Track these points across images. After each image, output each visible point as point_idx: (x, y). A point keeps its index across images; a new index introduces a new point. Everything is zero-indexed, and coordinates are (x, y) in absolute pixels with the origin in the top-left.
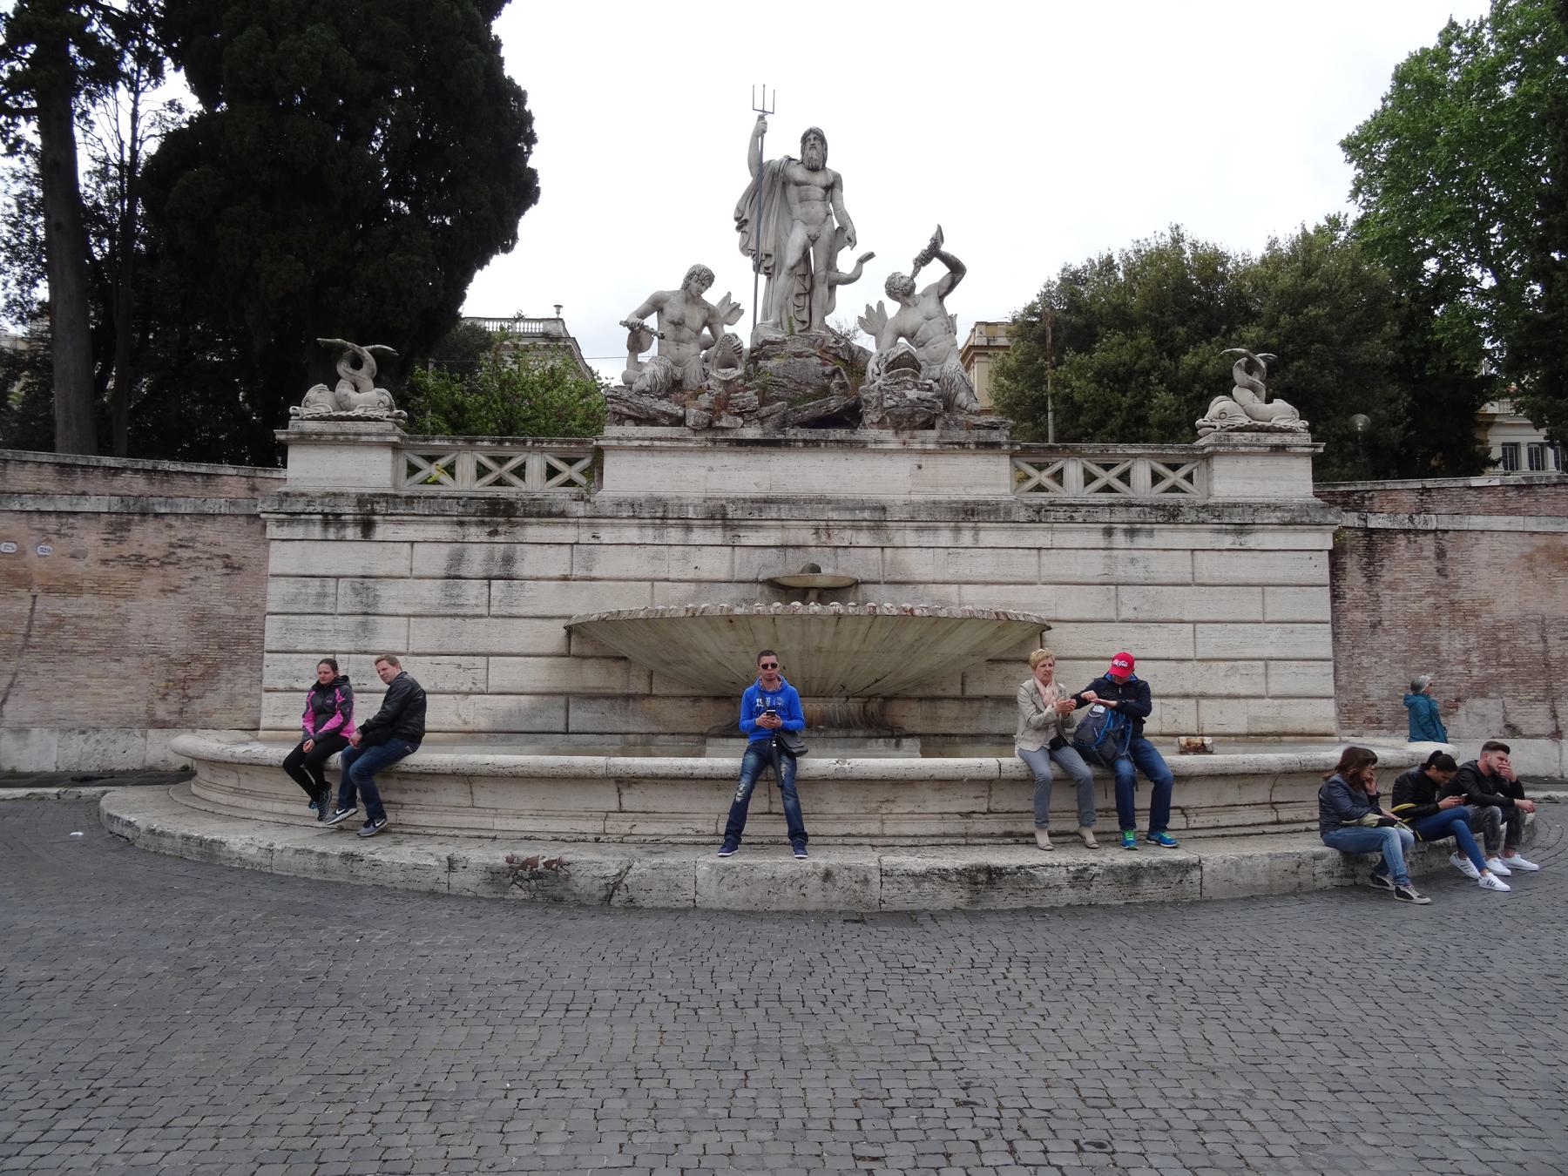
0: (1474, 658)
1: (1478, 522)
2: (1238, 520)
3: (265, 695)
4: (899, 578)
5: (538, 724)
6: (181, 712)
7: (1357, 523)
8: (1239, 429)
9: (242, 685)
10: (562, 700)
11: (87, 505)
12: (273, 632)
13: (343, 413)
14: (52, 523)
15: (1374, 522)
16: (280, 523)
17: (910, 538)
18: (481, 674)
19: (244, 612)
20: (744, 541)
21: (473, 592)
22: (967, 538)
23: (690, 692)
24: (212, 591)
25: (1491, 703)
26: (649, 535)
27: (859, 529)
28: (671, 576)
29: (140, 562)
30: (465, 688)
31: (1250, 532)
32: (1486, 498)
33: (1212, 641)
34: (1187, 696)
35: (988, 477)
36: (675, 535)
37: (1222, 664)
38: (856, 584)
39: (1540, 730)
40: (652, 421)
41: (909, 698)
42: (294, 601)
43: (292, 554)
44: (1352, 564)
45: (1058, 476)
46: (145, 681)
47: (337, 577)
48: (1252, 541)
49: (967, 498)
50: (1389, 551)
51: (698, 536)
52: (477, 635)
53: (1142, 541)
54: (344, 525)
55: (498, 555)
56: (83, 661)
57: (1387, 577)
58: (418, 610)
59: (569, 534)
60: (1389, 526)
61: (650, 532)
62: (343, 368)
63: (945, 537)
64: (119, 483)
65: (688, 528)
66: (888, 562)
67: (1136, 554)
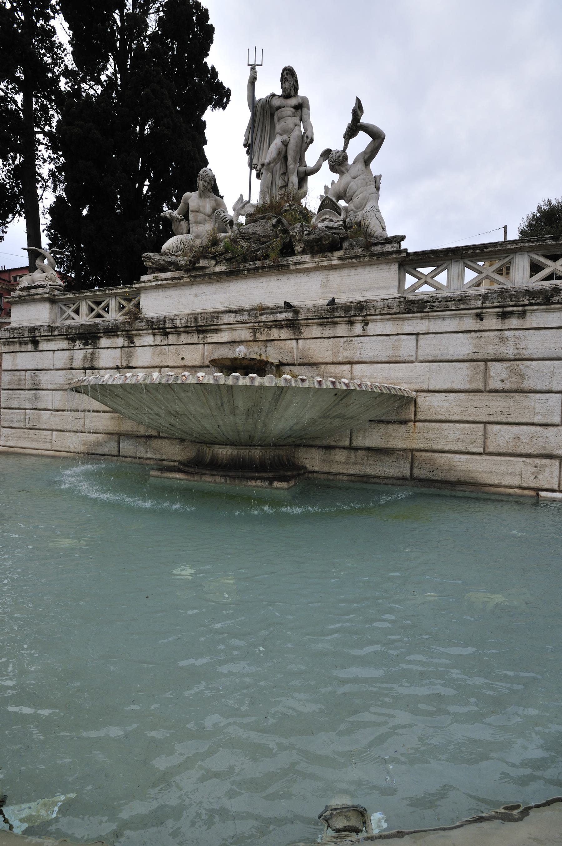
5: (104, 450)
10: (116, 437)
17: (315, 331)
20: (210, 340)
22: (358, 329)
26: (159, 340)
28: (170, 364)
36: (172, 339)
41: (311, 446)
42: (9, 383)
47: (26, 370)
49: (362, 299)
51: (184, 338)
53: (514, 322)
55: (89, 356)
58: (55, 387)
61: (159, 338)
65: (179, 334)
66: (300, 350)
67: (507, 333)
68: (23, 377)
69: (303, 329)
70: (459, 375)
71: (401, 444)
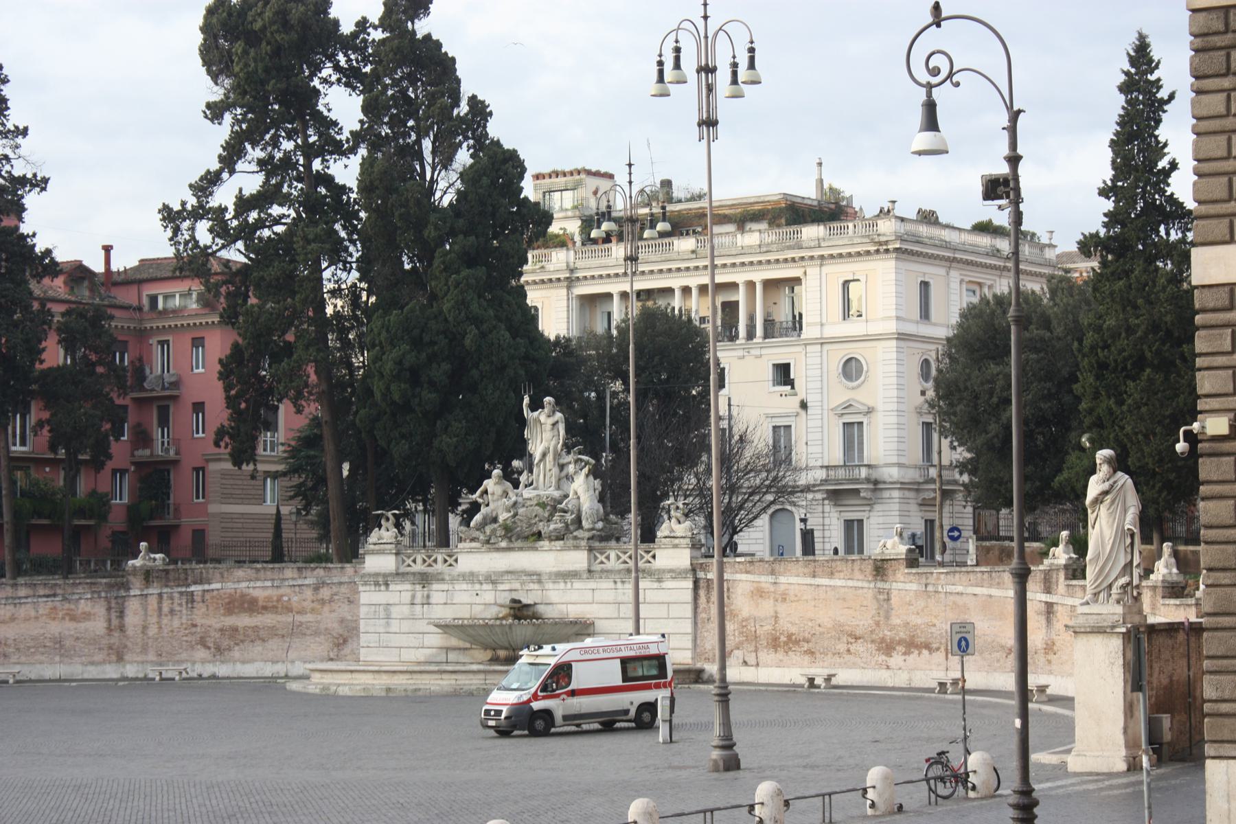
5: (438, 659)
9: (355, 644)
11: (307, 582)
12: (363, 626)
14: (297, 589)
17: (550, 586)
21: (418, 608)
22: (569, 585)
24: (344, 610)
35: (577, 559)
43: (369, 596)
44: (702, 593)
45: (608, 558)
48: (664, 585)
51: (485, 587)
59: (445, 587)
62: (383, 522)
63: (562, 585)
64: (315, 573)
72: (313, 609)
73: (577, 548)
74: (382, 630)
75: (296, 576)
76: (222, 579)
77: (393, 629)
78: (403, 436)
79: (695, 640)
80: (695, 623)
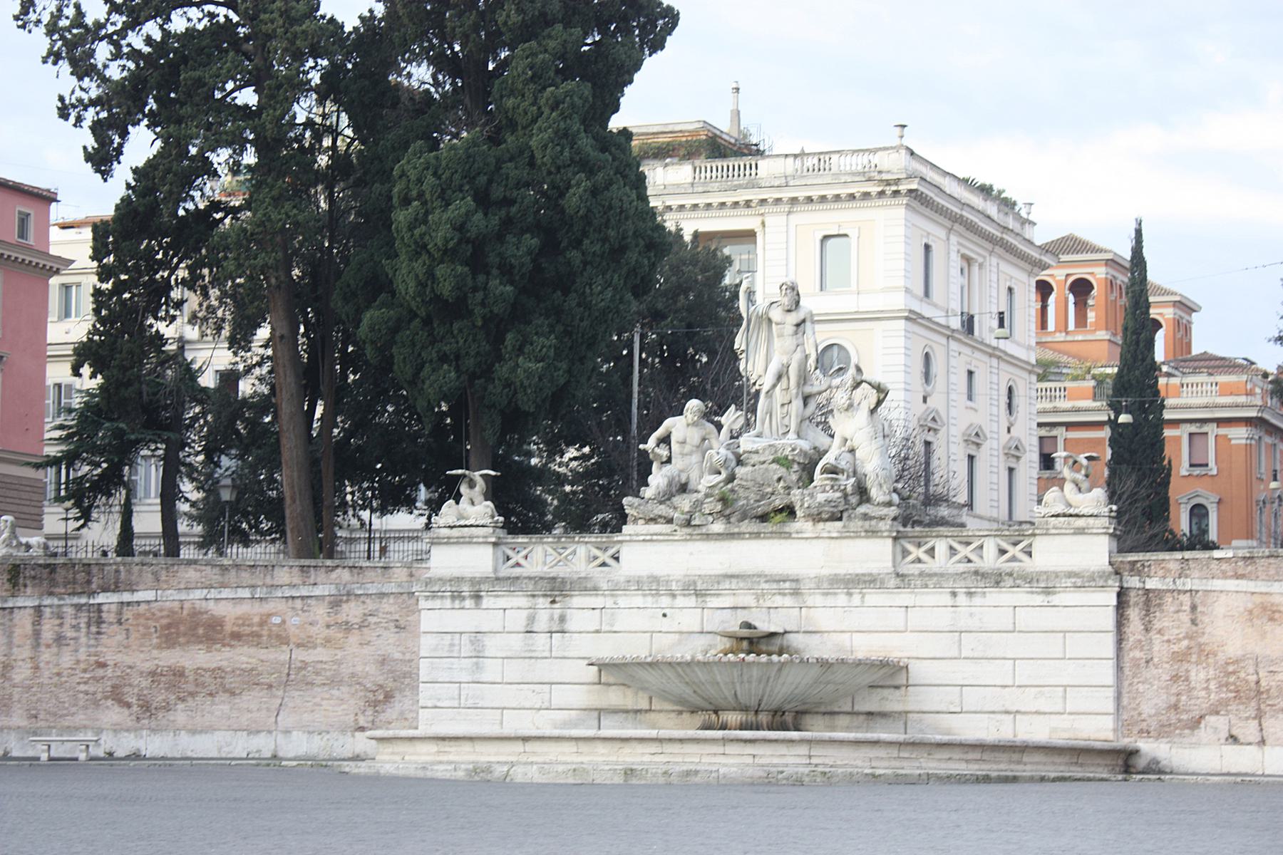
0: (1213, 686)
1: (1218, 584)
2: (1045, 584)
3: (421, 711)
4: (810, 629)
6: (373, 722)
7: (1139, 585)
8: (1058, 516)
9: (407, 703)
10: (596, 714)
11: (317, 591)
12: (425, 670)
13: (462, 523)
14: (298, 604)
15: (1150, 584)
16: (427, 598)
17: (818, 600)
18: (547, 697)
19: (408, 657)
20: (709, 605)
21: (541, 641)
22: (856, 599)
23: (675, 708)
24: (387, 643)
25: (1222, 719)
27: (784, 595)
29: (347, 627)
30: (537, 706)
31: (1054, 593)
32: (1224, 566)
33: (1025, 673)
34: (1007, 712)
35: (875, 554)
37: (1033, 689)
38: (786, 632)
39: (1251, 739)
40: (653, 520)
42: (435, 649)
43: (435, 618)
44: (1134, 614)
45: (931, 552)
46: (352, 702)
49: (860, 571)
50: (1159, 605)
51: (680, 601)
52: (543, 670)
53: (977, 600)
54: (464, 598)
55: (556, 617)
56: (319, 690)
57: (1157, 625)
58: (509, 654)
59: (598, 601)
60: (1160, 586)
61: (649, 599)
62: (464, 489)
63: (842, 599)
64: (334, 575)
65: (674, 596)
68: (457, 642)
69: (806, 598)
70: (943, 645)
71: (897, 707)
72: (328, 640)
73: (873, 533)
74: (465, 677)
75: (296, 580)
76: (157, 583)
77: (485, 677)
78: (443, 358)
79: (1118, 698)
80: (1119, 668)
